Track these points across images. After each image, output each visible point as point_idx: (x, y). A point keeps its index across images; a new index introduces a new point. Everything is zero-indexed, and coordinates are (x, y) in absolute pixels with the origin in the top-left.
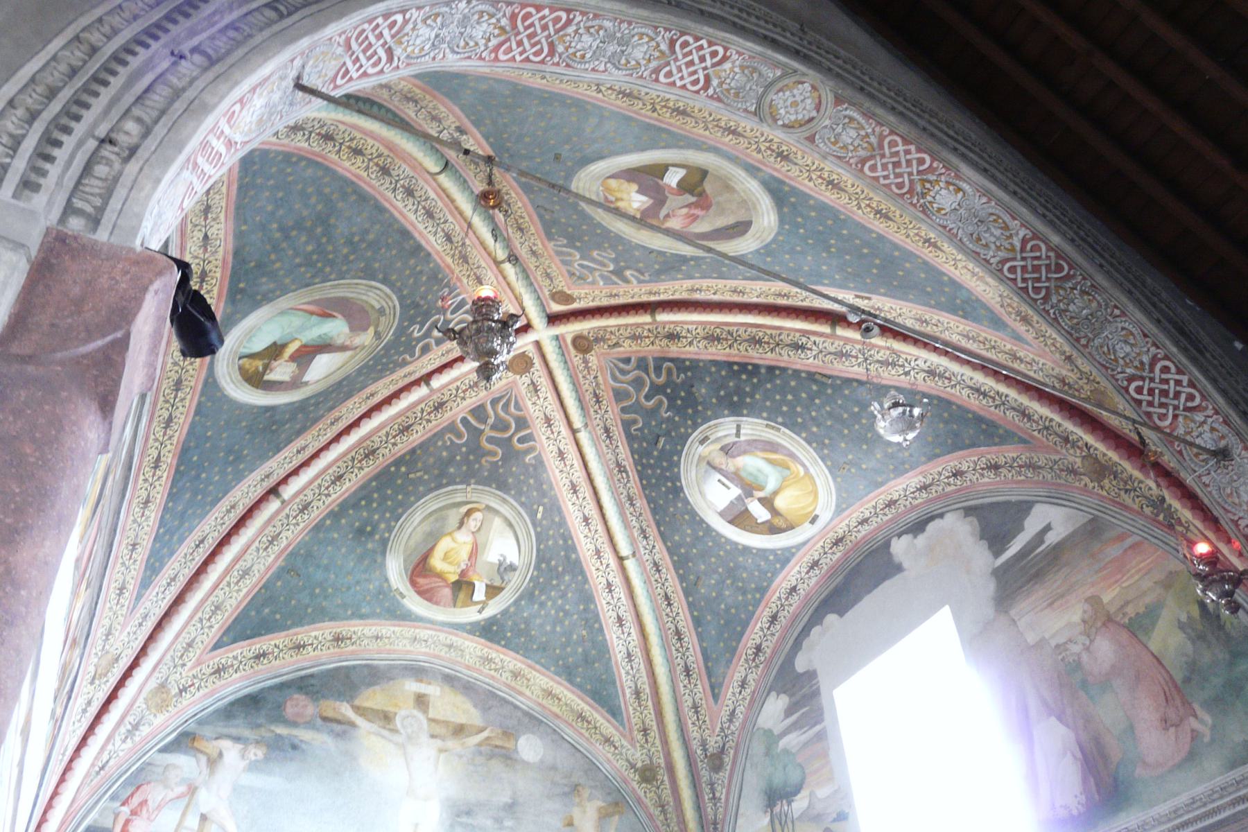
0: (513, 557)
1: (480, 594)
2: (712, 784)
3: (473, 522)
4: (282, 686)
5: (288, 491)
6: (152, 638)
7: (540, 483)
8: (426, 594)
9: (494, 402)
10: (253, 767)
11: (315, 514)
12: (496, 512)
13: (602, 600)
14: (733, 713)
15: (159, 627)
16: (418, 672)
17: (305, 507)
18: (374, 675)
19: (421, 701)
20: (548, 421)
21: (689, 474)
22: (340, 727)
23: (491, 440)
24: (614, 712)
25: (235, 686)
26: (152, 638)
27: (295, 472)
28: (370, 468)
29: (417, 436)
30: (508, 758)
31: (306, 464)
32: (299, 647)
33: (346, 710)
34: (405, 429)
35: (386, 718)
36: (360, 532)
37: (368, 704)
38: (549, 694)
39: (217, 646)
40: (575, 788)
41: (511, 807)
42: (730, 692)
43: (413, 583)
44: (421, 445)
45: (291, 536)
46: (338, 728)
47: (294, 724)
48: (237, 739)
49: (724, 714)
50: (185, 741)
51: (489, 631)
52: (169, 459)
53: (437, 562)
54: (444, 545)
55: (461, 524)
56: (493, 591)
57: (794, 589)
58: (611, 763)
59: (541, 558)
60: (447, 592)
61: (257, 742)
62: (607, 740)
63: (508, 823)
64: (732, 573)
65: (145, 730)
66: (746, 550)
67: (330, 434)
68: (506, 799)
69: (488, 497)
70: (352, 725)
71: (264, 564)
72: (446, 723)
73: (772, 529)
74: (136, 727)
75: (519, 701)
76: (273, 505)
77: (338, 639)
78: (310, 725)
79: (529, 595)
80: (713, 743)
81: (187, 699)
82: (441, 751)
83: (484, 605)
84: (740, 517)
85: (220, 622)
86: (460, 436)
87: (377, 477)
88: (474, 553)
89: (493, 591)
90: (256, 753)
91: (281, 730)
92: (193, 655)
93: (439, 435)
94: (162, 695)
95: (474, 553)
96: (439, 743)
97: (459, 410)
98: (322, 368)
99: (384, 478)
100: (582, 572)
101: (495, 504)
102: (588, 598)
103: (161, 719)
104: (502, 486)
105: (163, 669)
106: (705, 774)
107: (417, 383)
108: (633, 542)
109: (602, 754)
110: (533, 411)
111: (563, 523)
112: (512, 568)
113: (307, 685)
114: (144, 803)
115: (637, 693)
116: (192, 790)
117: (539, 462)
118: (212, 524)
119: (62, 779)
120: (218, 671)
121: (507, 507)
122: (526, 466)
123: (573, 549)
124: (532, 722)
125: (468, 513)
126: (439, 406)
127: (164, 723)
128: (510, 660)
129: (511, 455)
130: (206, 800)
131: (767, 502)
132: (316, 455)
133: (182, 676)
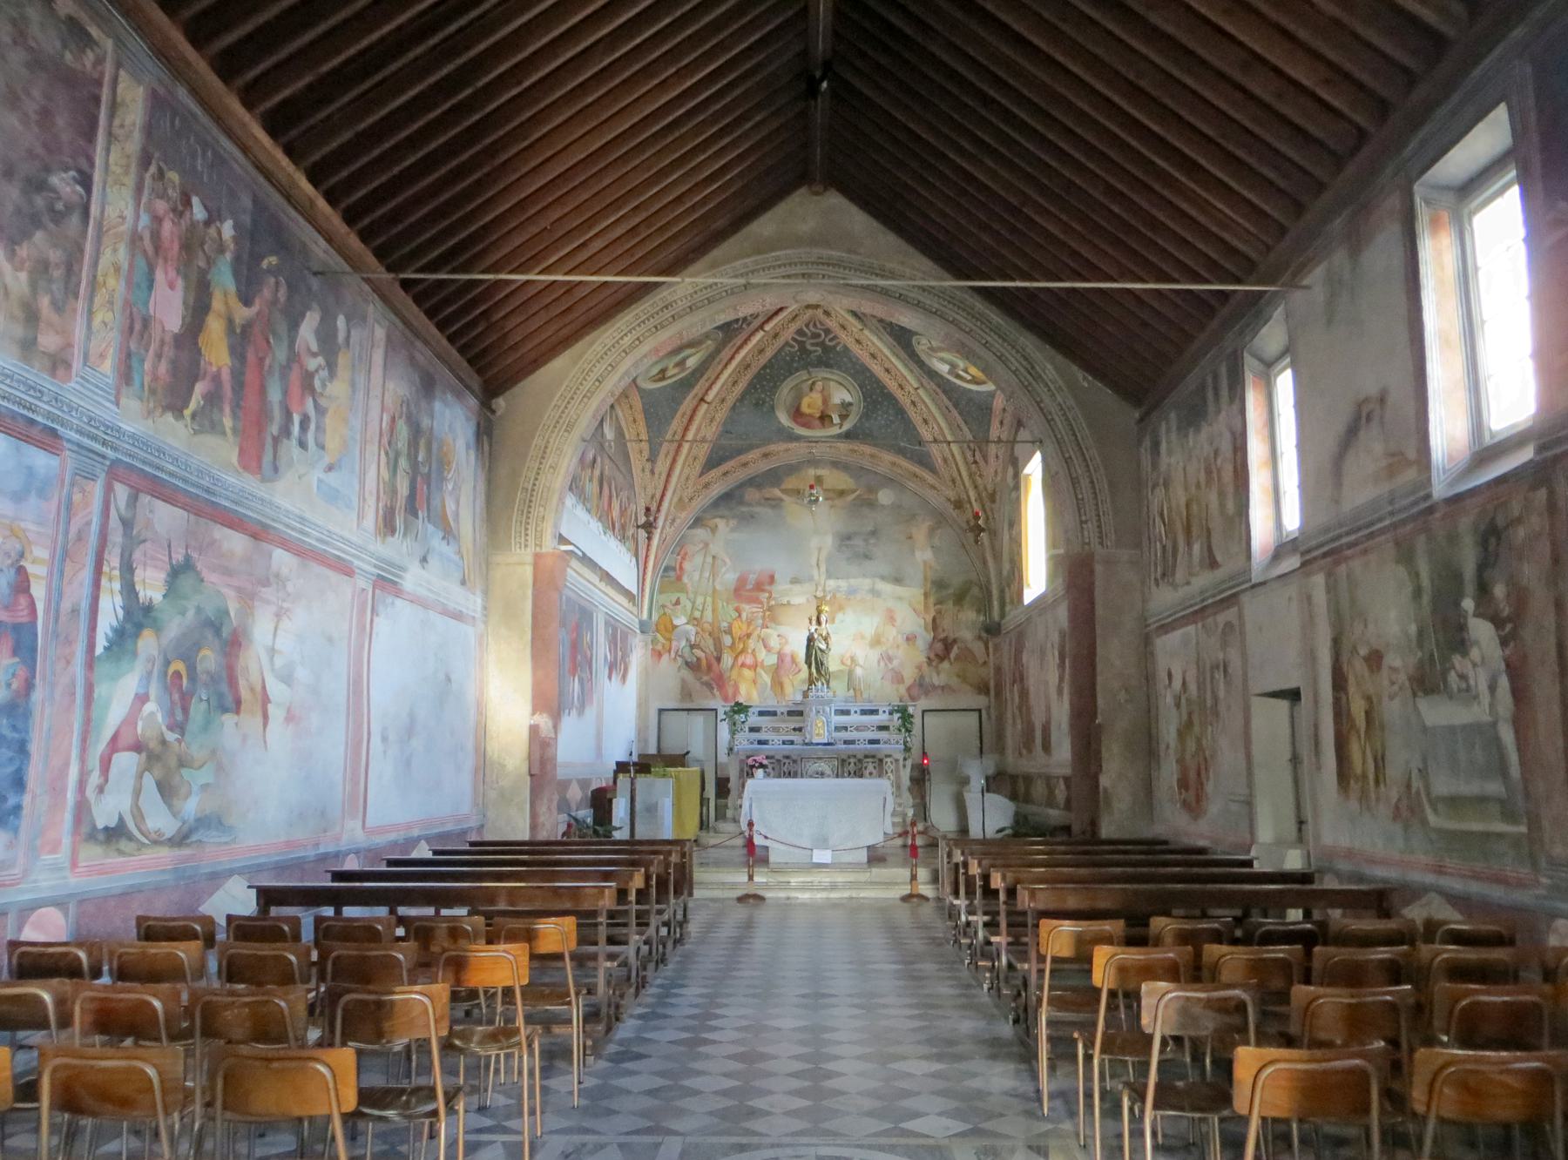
0: (848, 398)
1: (836, 420)
2: (992, 510)
3: (819, 385)
4: (742, 486)
5: (709, 398)
6: (667, 481)
7: (850, 359)
8: (806, 425)
9: (807, 326)
10: (733, 530)
11: (731, 400)
12: (830, 379)
13: (911, 412)
14: (996, 472)
15: (669, 476)
16: (814, 462)
17: (723, 400)
18: (792, 469)
19: (819, 480)
20: (843, 327)
21: (923, 357)
22: (775, 504)
23: (813, 345)
24: (933, 470)
25: (717, 490)
26: (667, 481)
27: (710, 388)
28: (749, 375)
29: (769, 353)
30: (872, 504)
31: (713, 383)
32: (745, 465)
33: (777, 492)
34: (761, 351)
35: (797, 493)
36: (757, 404)
37: (790, 487)
38: (894, 464)
39: (702, 474)
40: (914, 516)
41: (874, 533)
42: (992, 460)
43: (797, 422)
44: (775, 356)
45: (721, 416)
46: (773, 503)
47: (750, 505)
48: (721, 517)
49: (992, 470)
50: (698, 522)
51: (848, 436)
52: (640, 417)
53: (805, 409)
54: (805, 402)
55: (811, 390)
56: (843, 417)
57: (1004, 410)
58: (936, 500)
59: (866, 396)
60: (817, 422)
61: (733, 518)
62: (933, 487)
63: (872, 541)
64: (971, 400)
65: (678, 521)
66: (970, 390)
67: (720, 367)
68: (870, 528)
69: (822, 373)
70: (781, 500)
71: (711, 432)
72: (834, 491)
73: (975, 381)
74: (674, 520)
75: (880, 470)
76: (704, 407)
77: (766, 455)
78: (759, 504)
79: (866, 416)
80: (990, 488)
81: (694, 503)
82: (832, 507)
83: (841, 425)
84: (958, 376)
85: (698, 467)
86: (792, 347)
87: (755, 377)
88: (825, 401)
89: (843, 417)
90: (733, 523)
91: (744, 509)
92: (690, 482)
93: (782, 348)
94: (681, 504)
95: (825, 401)
96: (830, 502)
97: (788, 334)
98: (692, 363)
99: (759, 377)
100: (895, 399)
101: (829, 376)
102: (901, 412)
103: (683, 515)
104: (828, 366)
105: (678, 492)
106: (988, 505)
107: (757, 330)
108: (919, 380)
109: (930, 495)
110: (831, 324)
111: (873, 375)
112: (850, 404)
113: (754, 482)
114: (686, 554)
115: (945, 460)
116: (706, 545)
117: (845, 347)
118: (676, 425)
119: (648, 550)
120: (706, 486)
121: (835, 375)
122: (838, 353)
123: (884, 387)
124: (889, 481)
125: (814, 383)
126: (776, 336)
127: (686, 516)
128: (868, 449)
129: (826, 349)
130: (717, 547)
131: (966, 371)
132: (717, 378)
133: (690, 490)
